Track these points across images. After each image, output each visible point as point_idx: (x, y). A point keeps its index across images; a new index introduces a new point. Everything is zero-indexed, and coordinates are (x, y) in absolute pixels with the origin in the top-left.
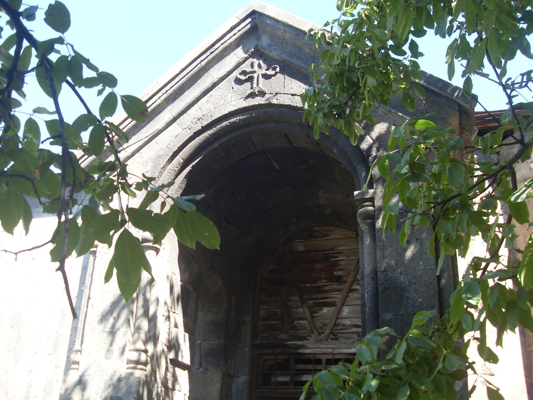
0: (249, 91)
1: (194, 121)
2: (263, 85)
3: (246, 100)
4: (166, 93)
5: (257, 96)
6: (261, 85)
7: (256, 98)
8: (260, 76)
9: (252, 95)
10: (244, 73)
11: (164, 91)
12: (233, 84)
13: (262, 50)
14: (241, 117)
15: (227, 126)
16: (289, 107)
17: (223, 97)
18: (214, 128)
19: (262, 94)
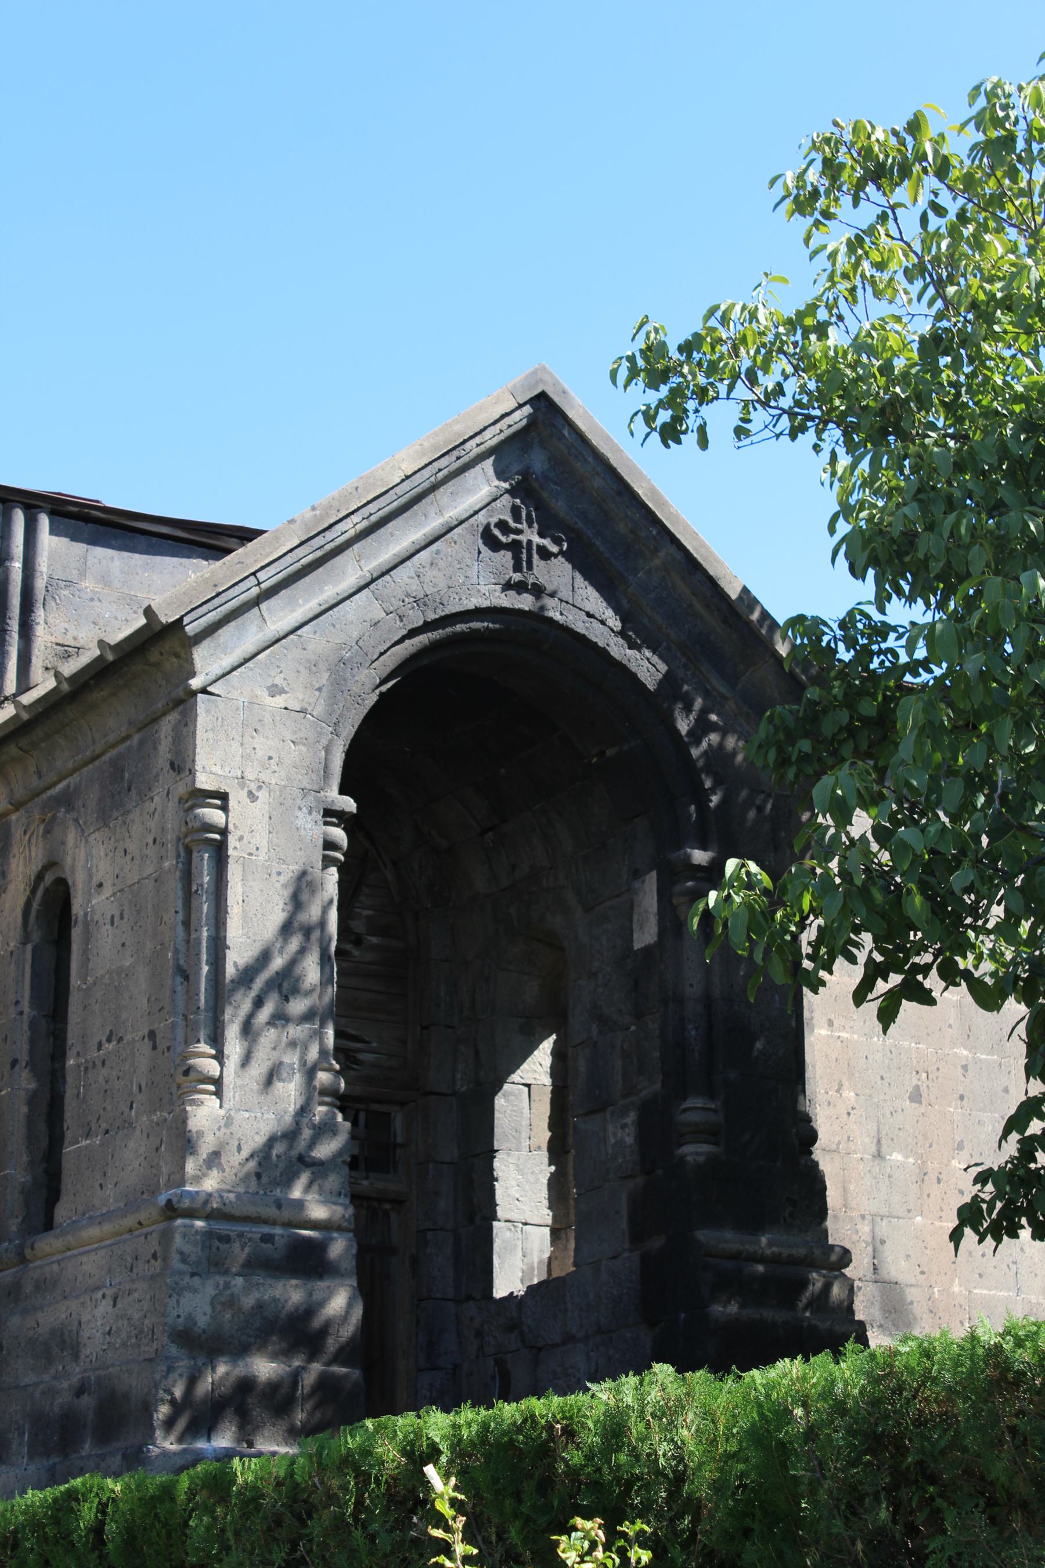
0: (517, 577)
1: (407, 600)
2: (542, 572)
3: (507, 592)
4: (368, 518)
5: (527, 591)
6: (535, 571)
7: (525, 595)
8: (535, 548)
9: (520, 587)
10: (502, 525)
11: (365, 512)
12: (480, 541)
13: (536, 485)
14: (490, 625)
15: (463, 632)
16: (582, 639)
17: (463, 566)
18: (440, 631)
19: (538, 591)
